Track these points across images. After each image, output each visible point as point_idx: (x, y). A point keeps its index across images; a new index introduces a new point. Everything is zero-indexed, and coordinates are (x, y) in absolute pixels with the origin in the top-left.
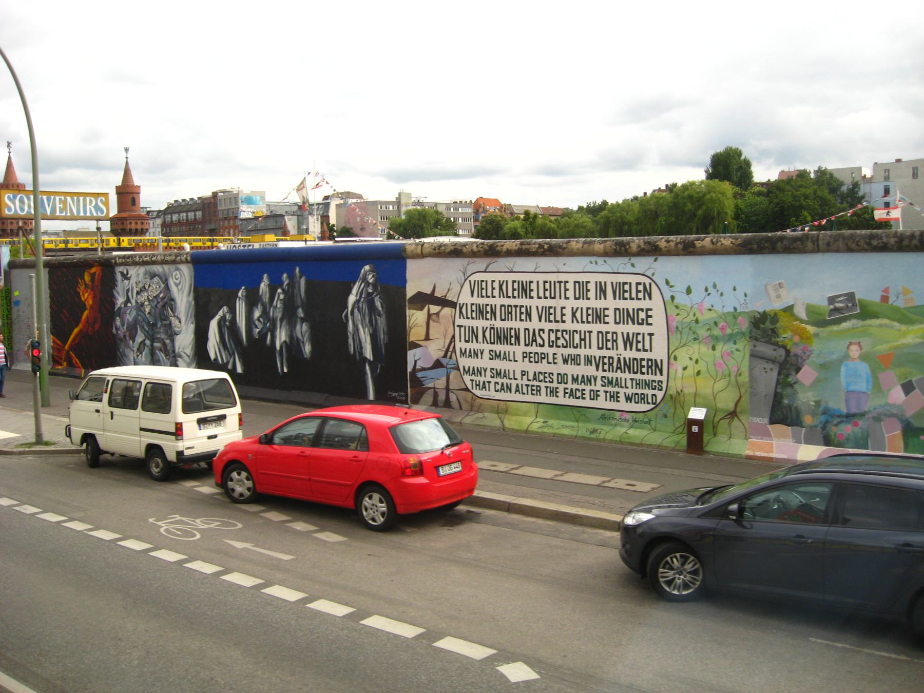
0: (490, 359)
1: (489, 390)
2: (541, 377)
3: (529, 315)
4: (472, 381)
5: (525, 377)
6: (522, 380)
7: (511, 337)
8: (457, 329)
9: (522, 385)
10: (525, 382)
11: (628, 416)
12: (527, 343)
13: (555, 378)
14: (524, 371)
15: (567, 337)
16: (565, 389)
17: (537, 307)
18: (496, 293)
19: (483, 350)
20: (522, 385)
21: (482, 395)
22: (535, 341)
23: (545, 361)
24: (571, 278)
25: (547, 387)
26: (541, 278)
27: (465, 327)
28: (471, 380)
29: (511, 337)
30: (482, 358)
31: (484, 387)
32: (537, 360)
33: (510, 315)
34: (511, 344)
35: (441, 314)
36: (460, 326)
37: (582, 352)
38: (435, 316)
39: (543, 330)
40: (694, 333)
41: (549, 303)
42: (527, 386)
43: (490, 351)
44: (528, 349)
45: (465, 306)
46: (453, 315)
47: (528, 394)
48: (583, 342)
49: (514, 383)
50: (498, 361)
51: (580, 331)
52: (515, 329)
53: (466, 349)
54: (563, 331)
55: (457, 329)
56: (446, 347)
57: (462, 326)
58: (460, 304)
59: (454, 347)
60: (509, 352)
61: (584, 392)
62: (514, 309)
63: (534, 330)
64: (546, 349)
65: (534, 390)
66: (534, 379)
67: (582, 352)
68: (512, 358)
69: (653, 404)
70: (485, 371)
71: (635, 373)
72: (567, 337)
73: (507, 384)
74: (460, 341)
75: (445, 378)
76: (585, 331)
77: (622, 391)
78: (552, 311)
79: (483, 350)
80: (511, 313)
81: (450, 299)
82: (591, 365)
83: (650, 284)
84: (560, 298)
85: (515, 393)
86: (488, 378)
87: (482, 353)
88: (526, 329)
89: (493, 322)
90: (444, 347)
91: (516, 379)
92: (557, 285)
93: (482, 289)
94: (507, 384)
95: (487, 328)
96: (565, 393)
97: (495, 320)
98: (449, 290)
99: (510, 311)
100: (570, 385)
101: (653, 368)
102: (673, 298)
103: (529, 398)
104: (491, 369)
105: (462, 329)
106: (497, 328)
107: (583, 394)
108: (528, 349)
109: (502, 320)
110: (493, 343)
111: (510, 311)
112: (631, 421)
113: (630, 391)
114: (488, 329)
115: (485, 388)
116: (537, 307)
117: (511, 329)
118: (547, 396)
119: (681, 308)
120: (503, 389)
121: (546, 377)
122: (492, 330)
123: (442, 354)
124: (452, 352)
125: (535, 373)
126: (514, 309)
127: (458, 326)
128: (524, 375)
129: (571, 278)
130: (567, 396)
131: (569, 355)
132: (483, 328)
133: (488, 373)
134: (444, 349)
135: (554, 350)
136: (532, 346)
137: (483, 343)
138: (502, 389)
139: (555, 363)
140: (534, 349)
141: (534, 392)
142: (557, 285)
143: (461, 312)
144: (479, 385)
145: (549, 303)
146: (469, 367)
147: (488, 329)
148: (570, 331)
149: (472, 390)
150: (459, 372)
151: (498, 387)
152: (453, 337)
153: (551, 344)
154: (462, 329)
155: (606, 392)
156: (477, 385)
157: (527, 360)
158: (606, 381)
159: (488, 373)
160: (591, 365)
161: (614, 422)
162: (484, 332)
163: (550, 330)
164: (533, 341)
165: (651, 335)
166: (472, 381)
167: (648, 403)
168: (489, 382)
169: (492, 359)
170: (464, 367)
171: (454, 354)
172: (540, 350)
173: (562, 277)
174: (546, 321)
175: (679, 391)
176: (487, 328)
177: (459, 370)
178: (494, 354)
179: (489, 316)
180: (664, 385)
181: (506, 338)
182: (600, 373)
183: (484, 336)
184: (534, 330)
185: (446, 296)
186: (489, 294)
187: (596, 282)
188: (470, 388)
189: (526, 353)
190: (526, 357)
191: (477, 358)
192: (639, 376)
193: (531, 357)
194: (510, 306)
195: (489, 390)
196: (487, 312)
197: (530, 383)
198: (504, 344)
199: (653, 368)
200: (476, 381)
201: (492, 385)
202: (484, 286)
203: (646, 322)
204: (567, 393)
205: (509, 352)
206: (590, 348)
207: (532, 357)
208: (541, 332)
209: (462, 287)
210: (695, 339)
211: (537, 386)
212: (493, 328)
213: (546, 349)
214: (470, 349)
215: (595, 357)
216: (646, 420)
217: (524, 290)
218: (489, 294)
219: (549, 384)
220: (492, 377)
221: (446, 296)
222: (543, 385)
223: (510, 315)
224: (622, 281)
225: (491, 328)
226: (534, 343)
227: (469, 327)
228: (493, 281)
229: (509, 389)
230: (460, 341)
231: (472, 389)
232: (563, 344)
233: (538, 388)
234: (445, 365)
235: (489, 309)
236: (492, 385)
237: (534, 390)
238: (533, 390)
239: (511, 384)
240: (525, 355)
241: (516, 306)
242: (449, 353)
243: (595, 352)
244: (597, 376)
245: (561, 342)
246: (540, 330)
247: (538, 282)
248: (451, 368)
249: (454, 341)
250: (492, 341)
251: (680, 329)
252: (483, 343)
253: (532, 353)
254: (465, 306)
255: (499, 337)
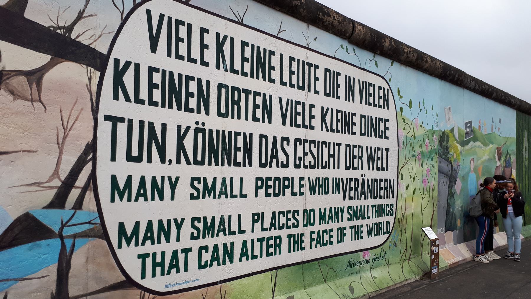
0: (192, 197)
1: (186, 270)
2: (283, 220)
3: (268, 110)
4: (143, 257)
5: (258, 225)
6: (253, 231)
7: (237, 149)
8: (105, 127)
9: (252, 241)
10: (259, 234)
11: (370, 255)
12: (264, 161)
13: (300, 218)
14: (258, 214)
15: (315, 151)
16: (312, 233)
17: (280, 99)
18: (210, 55)
19: (177, 179)
20: (252, 241)
21: (167, 286)
22: (276, 157)
23: (288, 191)
24: (323, 63)
25: (289, 236)
26: (289, 51)
27: (130, 121)
28: (139, 256)
29: (237, 149)
30: (172, 198)
31: (174, 265)
32: (277, 192)
33: (236, 107)
34: (237, 164)
35: (49, 77)
36: (114, 120)
37: (330, 174)
38: (23, 79)
39: (287, 139)
40: (413, 149)
41: (296, 95)
42: (261, 240)
43: (193, 179)
44: (265, 173)
45: (131, 70)
46: (94, 88)
47: (261, 256)
48: (332, 159)
49: (238, 240)
50: (209, 200)
51: (330, 143)
52: (245, 134)
53: (129, 179)
54: (312, 142)
55: (105, 127)
56: (64, 175)
57: (122, 120)
58: (117, 62)
59: (93, 176)
60: (232, 179)
61: (332, 234)
62: (243, 95)
63: (275, 138)
64: (291, 172)
65: (271, 246)
66: (272, 225)
67: (330, 174)
68: (236, 191)
69: (388, 232)
70: (179, 226)
71: (375, 198)
72: (315, 151)
73: (225, 245)
74: (113, 158)
75: (52, 271)
76: (334, 143)
77: (364, 222)
78: (300, 109)
79: (177, 179)
80: (238, 103)
81: (85, 40)
82: (339, 193)
83: (388, 90)
84: (309, 91)
85: (240, 260)
86: (186, 242)
87: (173, 187)
88: (262, 136)
89: (202, 117)
90: (56, 174)
91: (244, 232)
92: (307, 67)
93: (179, 40)
94: (225, 245)
95: (188, 128)
96: (312, 240)
97: (207, 113)
98: (80, 16)
99: (236, 99)
100: (318, 227)
101: (388, 189)
102: (401, 109)
103: (265, 263)
104: (193, 220)
105: (122, 128)
106: (211, 131)
107: (331, 237)
108: (265, 173)
109: (220, 114)
110: (202, 163)
111: (236, 99)
112: (371, 261)
113: (370, 222)
114: (191, 133)
115: (177, 267)
116: (280, 99)
117: (237, 134)
118: (289, 252)
119: (406, 122)
120: (217, 259)
121: (290, 219)
122: (200, 135)
123: (50, 195)
124: (84, 190)
125: (274, 213)
126: (243, 95)
127: (107, 118)
128: (257, 221)
129: (323, 63)
130: (314, 243)
131: (316, 178)
132: (179, 127)
133: (187, 230)
134: (57, 183)
135: (301, 172)
136: (270, 166)
137: (178, 162)
138: (213, 259)
139: (301, 194)
140: (274, 172)
141: (271, 250)
142: (307, 67)
143: (118, 83)
144: (162, 264)
145: (296, 95)
146: (137, 224)
147: (191, 133)
148: (319, 142)
149: (144, 283)
150: (105, 242)
151: (207, 257)
152: (92, 147)
153: (298, 163)
154: (122, 128)
155: (351, 227)
156: (155, 265)
157: (262, 192)
158: (351, 213)
159: (187, 230)
160: (339, 193)
161: (358, 267)
162: (181, 138)
163: (297, 140)
164: (273, 157)
165: (387, 150)
166: (143, 257)
167: (384, 233)
168: (186, 251)
169: (198, 197)
170: (121, 226)
171: (89, 195)
172: (282, 173)
173: (314, 58)
174: (291, 125)
175: (404, 213)
176: (188, 128)
177: (105, 236)
178: (201, 187)
179: (193, 103)
180: (394, 209)
181: (227, 151)
182: (348, 203)
183: (180, 147)
184: (275, 138)
185: (70, 29)
186: (196, 54)
187: (346, 76)
188: (136, 276)
189: (261, 179)
190: (261, 187)
191: (161, 198)
192: (378, 202)
193: (268, 187)
194: (238, 89)
195: (186, 270)
196: (189, 95)
197: (266, 234)
198: (223, 165)
199: (388, 189)
200: (154, 255)
201: (193, 257)
202: (183, 32)
203: (383, 136)
204: (314, 240)
205: (232, 179)
206: (338, 168)
207: (270, 187)
208: (285, 143)
209: (124, 21)
210: (414, 156)
211: (276, 237)
212: (203, 131)
213: (291, 172)
214: (143, 179)
215: (342, 179)
216: (382, 254)
217: (261, 64)
218: (196, 54)
219: (292, 231)
220: (193, 237)
221: (70, 29)
222: (284, 233)
223: (236, 107)
224: (368, 81)
225: (197, 131)
226: (274, 161)
227: (142, 123)
228: (204, 31)
229: (229, 254)
230: (113, 158)
231: (143, 277)
232: (310, 162)
233: (278, 241)
234: (56, 229)
235: (193, 87)
236: (193, 257)
237: (271, 246)
238: (269, 246)
239: (232, 244)
240: (260, 183)
241: (247, 92)
242: (74, 194)
243: (343, 174)
244: (344, 207)
245: (309, 158)
246: (283, 139)
247: (282, 55)
248: (75, 236)
249: (94, 159)
250: (199, 158)
251: (405, 145)
252: (178, 162)
253: (270, 179)
254: (131, 70)
255: (213, 151)
